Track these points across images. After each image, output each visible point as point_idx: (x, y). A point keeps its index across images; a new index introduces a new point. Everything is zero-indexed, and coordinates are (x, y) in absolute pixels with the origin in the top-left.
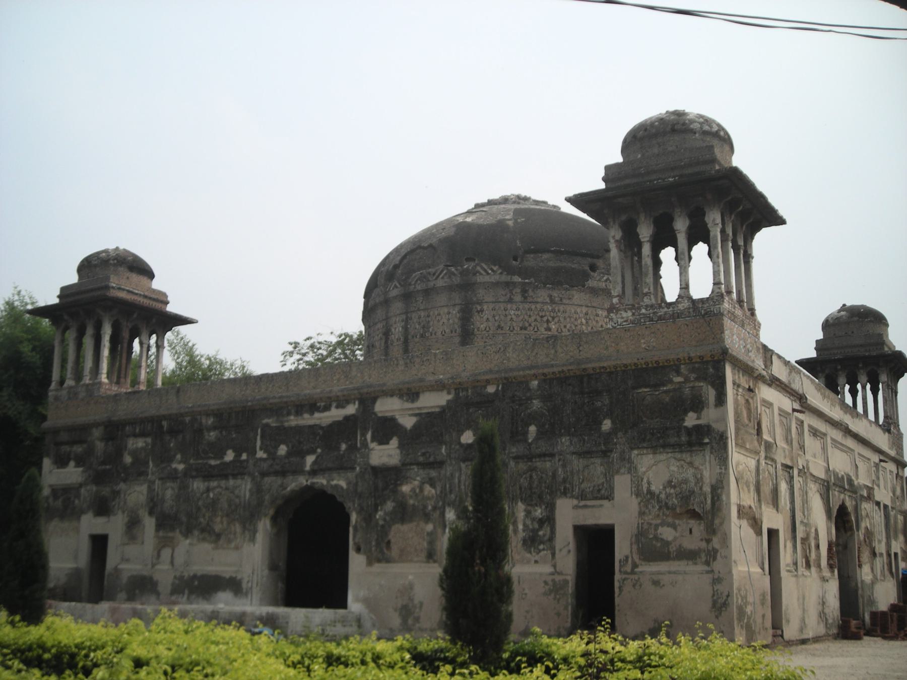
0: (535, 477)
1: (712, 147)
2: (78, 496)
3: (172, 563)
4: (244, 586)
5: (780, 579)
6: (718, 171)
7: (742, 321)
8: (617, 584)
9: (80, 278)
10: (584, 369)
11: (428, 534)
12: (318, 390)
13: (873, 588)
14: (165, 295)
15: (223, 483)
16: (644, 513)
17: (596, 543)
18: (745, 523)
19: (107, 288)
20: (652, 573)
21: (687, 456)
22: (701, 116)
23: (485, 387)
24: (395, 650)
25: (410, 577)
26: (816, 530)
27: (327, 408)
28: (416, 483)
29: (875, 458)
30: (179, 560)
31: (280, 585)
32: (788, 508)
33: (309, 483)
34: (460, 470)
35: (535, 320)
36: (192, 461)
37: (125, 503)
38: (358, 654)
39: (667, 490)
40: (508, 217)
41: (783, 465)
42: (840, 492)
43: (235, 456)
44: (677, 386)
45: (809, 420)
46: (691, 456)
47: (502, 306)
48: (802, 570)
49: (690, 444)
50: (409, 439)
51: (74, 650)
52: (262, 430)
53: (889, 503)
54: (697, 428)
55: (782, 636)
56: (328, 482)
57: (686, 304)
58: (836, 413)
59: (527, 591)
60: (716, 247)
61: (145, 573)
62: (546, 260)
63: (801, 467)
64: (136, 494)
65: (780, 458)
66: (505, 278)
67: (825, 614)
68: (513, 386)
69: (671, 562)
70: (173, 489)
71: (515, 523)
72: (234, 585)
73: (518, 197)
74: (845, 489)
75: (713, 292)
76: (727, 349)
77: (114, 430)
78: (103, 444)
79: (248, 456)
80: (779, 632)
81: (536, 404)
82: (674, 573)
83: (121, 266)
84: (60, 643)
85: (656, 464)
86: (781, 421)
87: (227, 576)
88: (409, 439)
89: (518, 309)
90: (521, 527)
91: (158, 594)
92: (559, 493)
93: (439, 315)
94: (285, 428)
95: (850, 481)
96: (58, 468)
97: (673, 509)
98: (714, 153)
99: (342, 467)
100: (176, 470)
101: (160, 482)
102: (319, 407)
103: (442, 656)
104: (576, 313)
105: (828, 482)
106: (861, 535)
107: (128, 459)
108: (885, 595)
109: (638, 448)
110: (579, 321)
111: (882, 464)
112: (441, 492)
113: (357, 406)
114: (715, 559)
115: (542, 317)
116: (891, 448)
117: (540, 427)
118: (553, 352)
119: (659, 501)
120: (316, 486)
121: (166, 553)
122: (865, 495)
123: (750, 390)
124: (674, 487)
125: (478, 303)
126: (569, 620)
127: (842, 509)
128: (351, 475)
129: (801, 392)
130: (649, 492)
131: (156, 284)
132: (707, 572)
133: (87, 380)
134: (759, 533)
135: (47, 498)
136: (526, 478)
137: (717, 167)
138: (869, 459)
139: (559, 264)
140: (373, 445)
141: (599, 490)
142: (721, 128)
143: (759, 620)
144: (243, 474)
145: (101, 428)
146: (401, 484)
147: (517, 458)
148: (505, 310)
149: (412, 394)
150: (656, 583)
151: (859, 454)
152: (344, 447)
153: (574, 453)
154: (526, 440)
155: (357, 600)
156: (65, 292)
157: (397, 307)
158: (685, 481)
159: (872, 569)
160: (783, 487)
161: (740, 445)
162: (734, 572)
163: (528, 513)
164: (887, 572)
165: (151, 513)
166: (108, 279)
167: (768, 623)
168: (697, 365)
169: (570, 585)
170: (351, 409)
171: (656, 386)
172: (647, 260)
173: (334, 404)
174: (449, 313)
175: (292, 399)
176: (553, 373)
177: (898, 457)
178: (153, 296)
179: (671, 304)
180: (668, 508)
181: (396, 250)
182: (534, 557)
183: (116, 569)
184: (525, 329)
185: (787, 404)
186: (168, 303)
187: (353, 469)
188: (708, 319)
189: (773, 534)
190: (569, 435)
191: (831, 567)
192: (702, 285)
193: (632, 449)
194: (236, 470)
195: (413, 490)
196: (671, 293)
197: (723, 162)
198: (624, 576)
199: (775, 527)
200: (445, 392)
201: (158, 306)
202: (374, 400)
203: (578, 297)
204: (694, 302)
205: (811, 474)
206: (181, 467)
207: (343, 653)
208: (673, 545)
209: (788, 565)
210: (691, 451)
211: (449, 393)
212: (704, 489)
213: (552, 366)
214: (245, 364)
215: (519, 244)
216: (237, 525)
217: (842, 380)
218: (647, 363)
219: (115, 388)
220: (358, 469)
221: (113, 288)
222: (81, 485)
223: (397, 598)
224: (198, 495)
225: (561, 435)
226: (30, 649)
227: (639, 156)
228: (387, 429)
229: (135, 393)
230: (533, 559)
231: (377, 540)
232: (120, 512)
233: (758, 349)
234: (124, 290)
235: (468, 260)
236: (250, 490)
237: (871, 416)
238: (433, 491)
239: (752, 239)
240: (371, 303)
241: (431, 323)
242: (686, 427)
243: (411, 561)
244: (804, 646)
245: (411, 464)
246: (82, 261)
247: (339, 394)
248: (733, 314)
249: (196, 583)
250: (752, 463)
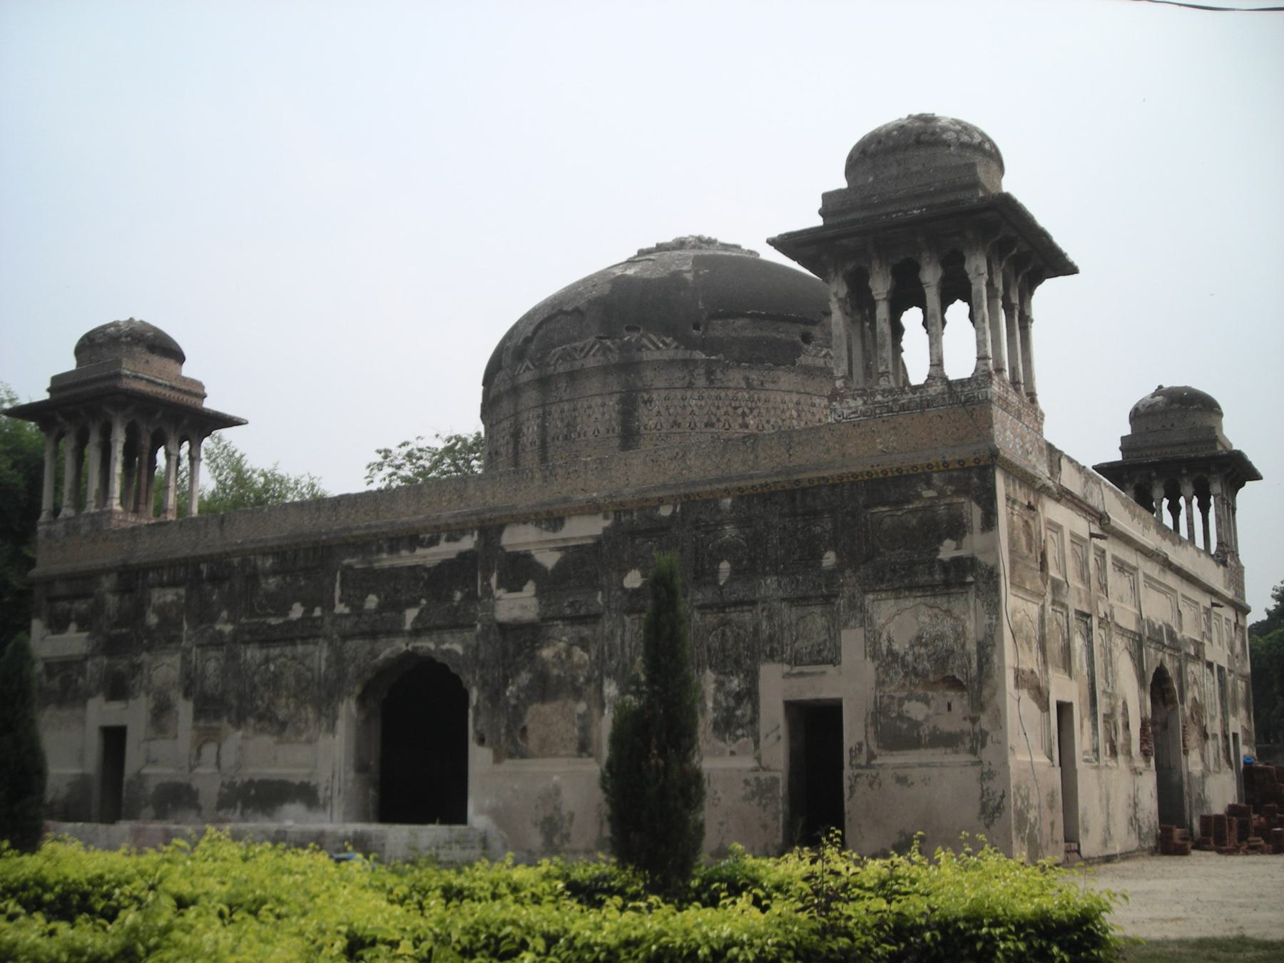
0: (729, 634)
1: (974, 165)
2: (82, 672)
3: (218, 764)
4: (321, 794)
5: (1075, 771)
6: (982, 199)
7: (1019, 410)
8: (846, 783)
9: (78, 365)
10: (798, 481)
11: (580, 716)
12: (421, 517)
13: (1203, 783)
14: (200, 385)
15: (288, 650)
16: (883, 683)
17: (816, 726)
18: (1024, 694)
19: (118, 376)
20: (895, 767)
22: (958, 122)
23: (657, 508)
24: (539, 878)
25: (556, 778)
26: (1125, 703)
27: (434, 542)
28: (562, 645)
29: (1206, 601)
30: (229, 759)
31: (372, 792)
32: (1085, 672)
33: (410, 648)
34: (624, 626)
35: (726, 413)
36: (243, 620)
37: (150, 681)
38: (486, 885)
39: (916, 649)
40: (685, 268)
41: (1077, 612)
42: (1157, 649)
43: (305, 612)
44: (928, 503)
45: (1112, 548)
46: (949, 602)
47: (679, 394)
48: (1105, 758)
49: (947, 584)
50: (550, 584)
51: (87, 887)
52: (342, 574)
53: (1225, 664)
54: (957, 561)
55: (1078, 851)
56: (437, 646)
57: (938, 387)
58: (1151, 539)
59: (720, 794)
60: (980, 307)
61: (181, 780)
62: (741, 328)
63: (1102, 615)
64: (165, 668)
65: (1074, 603)
66: (681, 354)
67: (1137, 820)
68: (696, 508)
69: (922, 750)
70: (217, 660)
71: (703, 697)
72: (307, 794)
73: (700, 239)
74: (1164, 646)
75: (976, 370)
76: (997, 450)
77: (133, 579)
78: (116, 599)
79: (323, 611)
80: (1074, 846)
81: (730, 531)
82: (927, 765)
83: (137, 344)
84: (66, 878)
85: (899, 613)
86: (1073, 549)
87: (297, 781)
88: (550, 584)
89: (701, 398)
90: (710, 704)
91: (199, 808)
92: (763, 657)
93: (590, 407)
94: (375, 571)
95: (1171, 634)
96: (53, 633)
97: (924, 675)
98: (976, 174)
99: (457, 624)
100: (221, 633)
102: (423, 540)
103: (606, 885)
104: (783, 402)
105: (1140, 636)
106: (1186, 709)
107: (152, 619)
108: (1221, 792)
109: (874, 591)
110: (788, 414)
111: (1215, 609)
112: (597, 657)
113: (476, 538)
114: (983, 745)
115: (735, 408)
116: (1227, 588)
117: (735, 563)
118: (752, 457)
119: (904, 666)
120: (420, 652)
121: (209, 751)
122: (1192, 653)
123: (1030, 507)
124: (926, 645)
125: (645, 390)
126: (781, 834)
127: (1161, 673)
128: (469, 636)
129: (1101, 509)
130: (891, 652)
131: (188, 370)
132: (974, 764)
133: (92, 508)
134: (1045, 707)
136: (716, 636)
137: (981, 194)
138: (1197, 603)
139: (758, 333)
140: (499, 593)
141: (820, 652)
142: (986, 138)
143: (1046, 830)
144: (317, 636)
145: (114, 577)
146: (541, 647)
147: (702, 608)
148: (683, 399)
149: (553, 520)
150: (902, 780)
151: (1183, 596)
152: (458, 595)
153: (783, 600)
154: (716, 582)
155: (481, 811)
156: (58, 384)
157: (530, 397)
158: (941, 637)
159: (1203, 757)
160: (1078, 643)
161: (1017, 585)
162: (1011, 763)
163: (720, 685)
164: (1222, 760)
165: (187, 695)
166: (119, 363)
167: (1059, 834)
168: (955, 474)
169: (781, 784)
170: (468, 543)
171: (898, 504)
172: (883, 326)
173: (444, 536)
174: (603, 405)
175: (384, 530)
176: (753, 487)
177: (1237, 600)
178: (184, 387)
179: (917, 388)
180: (917, 675)
181: (528, 317)
182: (729, 746)
183: (139, 775)
184: (712, 425)
185: (1082, 526)
186: (204, 396)
187: (473, 626)
188: (970, 408)
189: (1064, 709)
190: (776, 574)
191: (1145, 754)
192: (960, 364)
193: (865, 592)
194: (307, 632)
195: (558, 655)
196: (917, 372)
197: (989, 187)
198: (856, 772)
199: (1066, 699)
200: (601, 516)
201: (191, 401)
202: (500, 529)
203: (786, 379)
204: (950, 384)
205: (1117, 625)
206: (228, 628)
207: (466, 884)
208: (925, 727)
209: (1085, 752)
210: (948, 594)
211: (606, 517)
212: (968, 647)
213: (751, 477)
214: (315, 481)
215: (701, 305)
216: (310, 709)
217: (1158, 492)
218: (885, 472)
219: (132, 519)
220: (479, 626)
221: (127, 376)
222: (86, 658)
223: (537, 807)
224: (253, 668)
225: (765, 574)
226: (24, 887)
227: (871, 179)
228: (518, 569)
229: (160, 524)
230: (728, 749)
231: (508, 727)
232: (143, 694)
233: (1041, 450)
234: (142, 379)
235: (628, 329)
236: (327, 660)
237: (1200, 543)
238: (586, 656)
239: (1031, 294)
240: (493, 392)
241: (579, 420)
242: (941, 560)
243: (556, 755)
244: (1109, 866)
245: (556, 619)
246: (82, 339)
247: (451, 521)
248: (1005, 400)
249: (253, 792)
250: (1034, 610)
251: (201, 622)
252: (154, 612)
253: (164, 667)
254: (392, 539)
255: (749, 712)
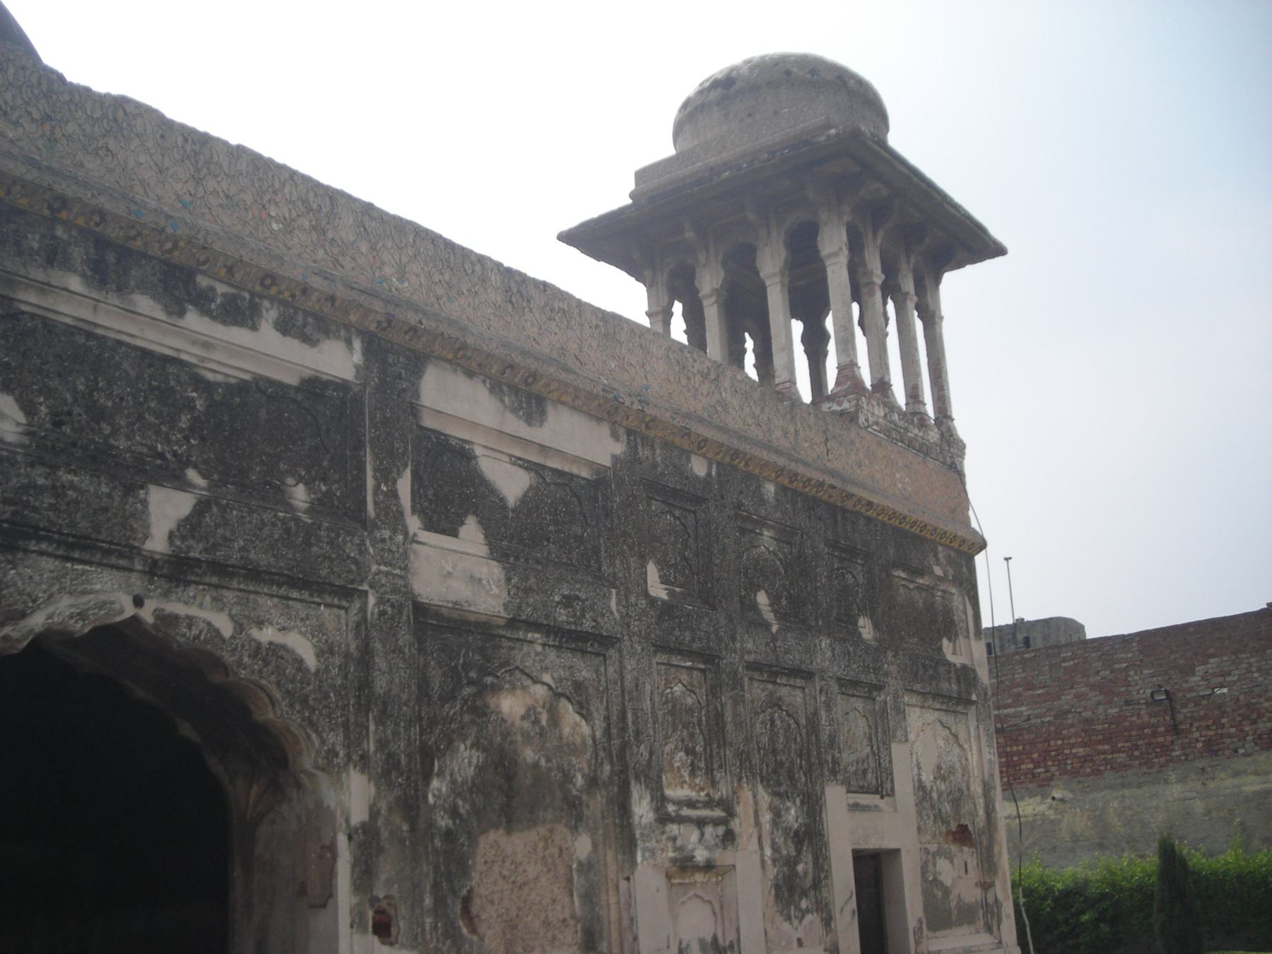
21: (949, 719)
27: (238, 312)
28: (540, 691)
33: (147, 614)
50: (515, 537)
56: (239, 627)
99: (306, 578)
112: (607, 731)
113: (358, 357)
120: (184, 635)
128: (337, 622)
140: (414, 523)
146: (496, 689)
152: (300, 495)
154: (767, 626)
158: (952, 770)
170: (338, 361)
173: (270, 314)
202: (417, 363)
220: (372, 600)
231: (436, 886)
238: (585, 729)
247: (316, 282)
254: (102, 243)
255: (810, 867)
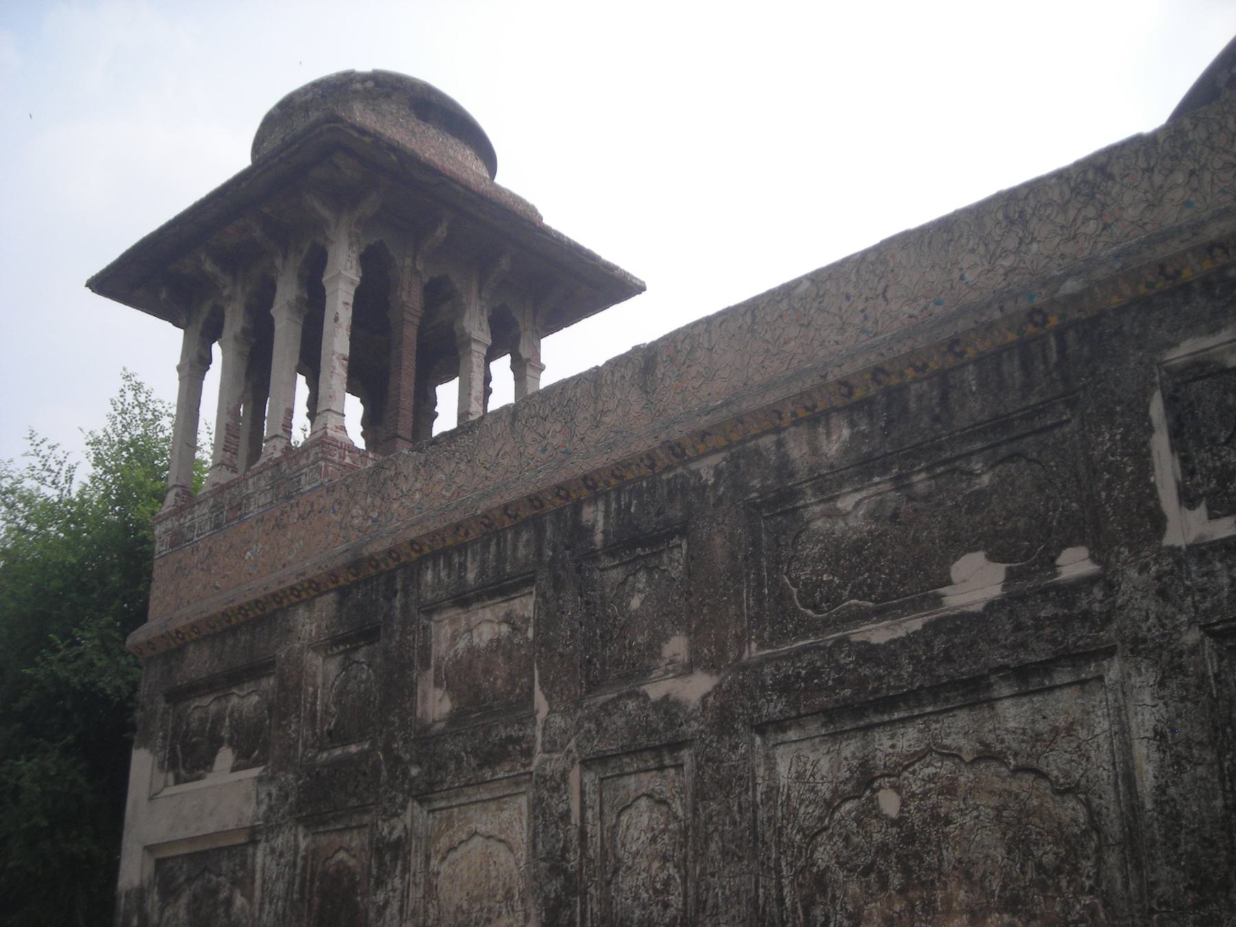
2: (243, 882)
15: (958, 729)
36: (753, 651)
37: (431, 890)
52: (1170, 402)
78: (333, 666)
83: (388, 96)
96: (178, 781)
100: (668, 706)
101: (590, 778)
107: (435, 704)
135: (141, 893)
145: (326, 604)
206: (696, 688)
222: (253, 835)
224: (808, 813)
251: (594, 686)
252: (437, 684)
253: (477, 840)
